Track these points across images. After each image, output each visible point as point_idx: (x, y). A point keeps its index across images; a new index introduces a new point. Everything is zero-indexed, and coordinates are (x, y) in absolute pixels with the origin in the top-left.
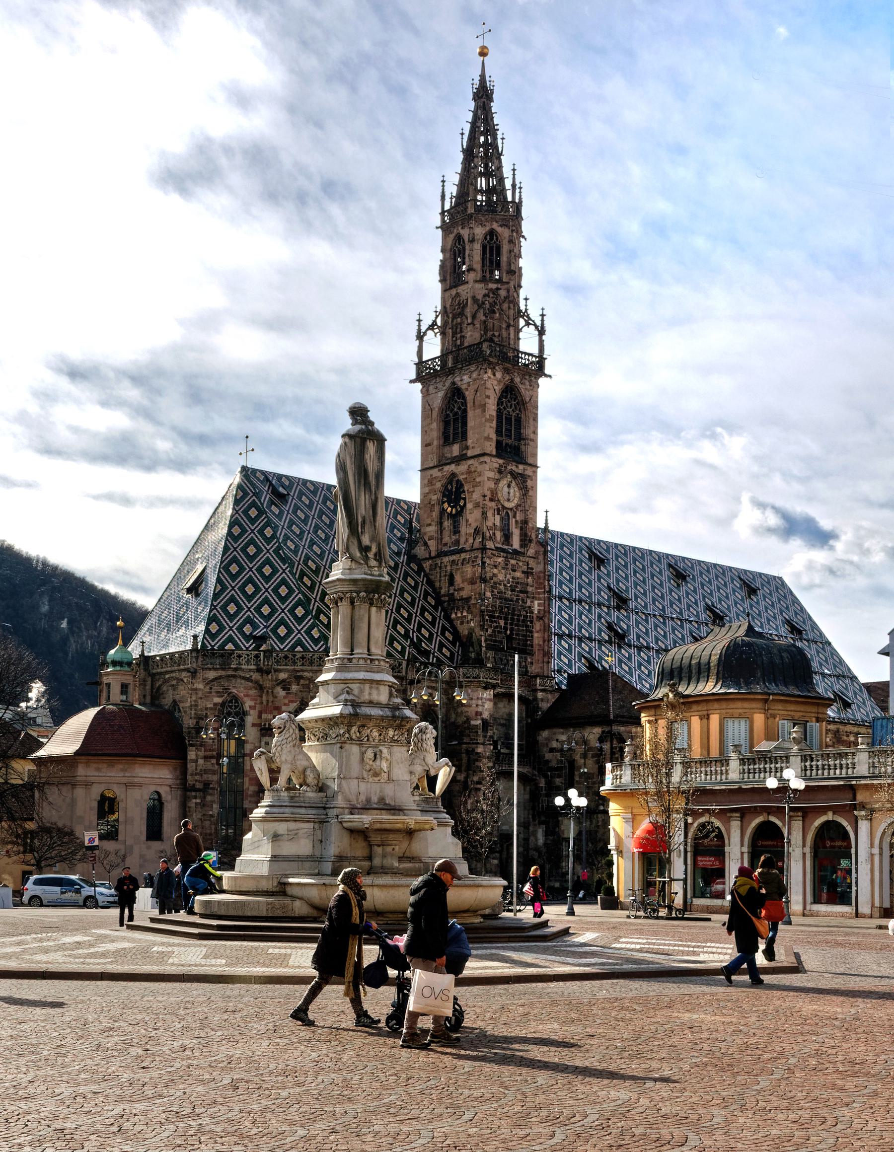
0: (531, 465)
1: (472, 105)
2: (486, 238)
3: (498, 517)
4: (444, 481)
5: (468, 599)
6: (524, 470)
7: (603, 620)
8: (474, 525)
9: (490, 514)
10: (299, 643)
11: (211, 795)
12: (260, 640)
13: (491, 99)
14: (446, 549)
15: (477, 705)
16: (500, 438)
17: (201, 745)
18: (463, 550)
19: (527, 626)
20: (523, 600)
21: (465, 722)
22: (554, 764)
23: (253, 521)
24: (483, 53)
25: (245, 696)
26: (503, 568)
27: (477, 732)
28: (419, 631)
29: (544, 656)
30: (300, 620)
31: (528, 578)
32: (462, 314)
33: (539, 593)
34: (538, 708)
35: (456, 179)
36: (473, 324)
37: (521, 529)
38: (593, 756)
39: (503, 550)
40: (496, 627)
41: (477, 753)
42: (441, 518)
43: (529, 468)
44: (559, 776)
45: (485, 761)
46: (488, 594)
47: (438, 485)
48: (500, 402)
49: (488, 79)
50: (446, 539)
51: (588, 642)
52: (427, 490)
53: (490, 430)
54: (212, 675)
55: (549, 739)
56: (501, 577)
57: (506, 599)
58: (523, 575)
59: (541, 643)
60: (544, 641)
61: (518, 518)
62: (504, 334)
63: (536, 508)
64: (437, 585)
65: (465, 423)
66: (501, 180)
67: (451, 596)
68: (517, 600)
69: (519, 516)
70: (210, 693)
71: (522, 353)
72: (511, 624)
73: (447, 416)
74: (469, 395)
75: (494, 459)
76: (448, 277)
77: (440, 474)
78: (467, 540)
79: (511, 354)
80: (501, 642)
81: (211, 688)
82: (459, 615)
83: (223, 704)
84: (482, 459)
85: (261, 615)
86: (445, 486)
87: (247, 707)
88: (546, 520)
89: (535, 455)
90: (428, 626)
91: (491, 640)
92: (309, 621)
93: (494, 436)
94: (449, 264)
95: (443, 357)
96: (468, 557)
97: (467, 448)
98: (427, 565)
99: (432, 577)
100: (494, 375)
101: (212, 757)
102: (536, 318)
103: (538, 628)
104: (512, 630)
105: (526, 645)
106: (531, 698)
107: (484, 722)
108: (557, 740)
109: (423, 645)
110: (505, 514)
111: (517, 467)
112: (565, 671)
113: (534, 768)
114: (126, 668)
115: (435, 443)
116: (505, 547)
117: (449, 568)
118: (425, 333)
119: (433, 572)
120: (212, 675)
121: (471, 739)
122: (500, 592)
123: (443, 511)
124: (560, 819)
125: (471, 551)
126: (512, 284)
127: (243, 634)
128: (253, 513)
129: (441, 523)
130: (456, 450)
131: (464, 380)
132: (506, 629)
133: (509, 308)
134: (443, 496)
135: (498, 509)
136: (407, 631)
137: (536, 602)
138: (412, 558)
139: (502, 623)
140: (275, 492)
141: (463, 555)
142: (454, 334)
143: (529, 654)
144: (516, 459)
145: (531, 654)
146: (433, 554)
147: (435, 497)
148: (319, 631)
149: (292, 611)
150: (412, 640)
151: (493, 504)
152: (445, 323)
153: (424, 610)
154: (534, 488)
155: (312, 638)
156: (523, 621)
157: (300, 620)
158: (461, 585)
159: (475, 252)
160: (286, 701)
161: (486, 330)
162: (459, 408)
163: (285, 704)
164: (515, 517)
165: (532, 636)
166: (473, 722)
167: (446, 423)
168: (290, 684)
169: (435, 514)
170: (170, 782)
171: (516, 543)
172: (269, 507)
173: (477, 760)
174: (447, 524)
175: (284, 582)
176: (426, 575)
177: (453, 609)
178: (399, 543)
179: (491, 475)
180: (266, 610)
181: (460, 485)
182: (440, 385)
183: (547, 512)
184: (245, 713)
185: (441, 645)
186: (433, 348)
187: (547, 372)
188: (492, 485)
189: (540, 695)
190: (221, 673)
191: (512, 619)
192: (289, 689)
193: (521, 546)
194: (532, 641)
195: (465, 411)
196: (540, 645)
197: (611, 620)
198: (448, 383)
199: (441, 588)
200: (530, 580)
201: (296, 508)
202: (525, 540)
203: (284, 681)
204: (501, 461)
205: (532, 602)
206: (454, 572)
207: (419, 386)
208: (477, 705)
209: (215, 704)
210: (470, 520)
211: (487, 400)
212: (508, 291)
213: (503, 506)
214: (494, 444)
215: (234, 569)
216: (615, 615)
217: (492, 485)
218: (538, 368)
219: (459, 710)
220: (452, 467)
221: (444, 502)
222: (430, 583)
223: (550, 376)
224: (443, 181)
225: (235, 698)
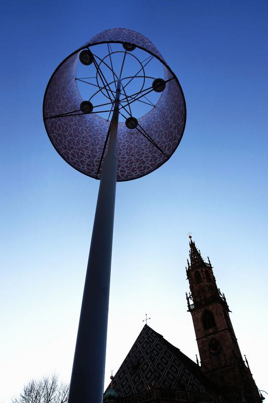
13: (194, 245)
24: (190, 237)
52: (201, 346)
74: (214, 312)
77: (206, 339)
97: (218, 328)
115: (202, 329)
130: (211, 331)
182: (200, 311)
198: (203, 310)
221: (210, 350)
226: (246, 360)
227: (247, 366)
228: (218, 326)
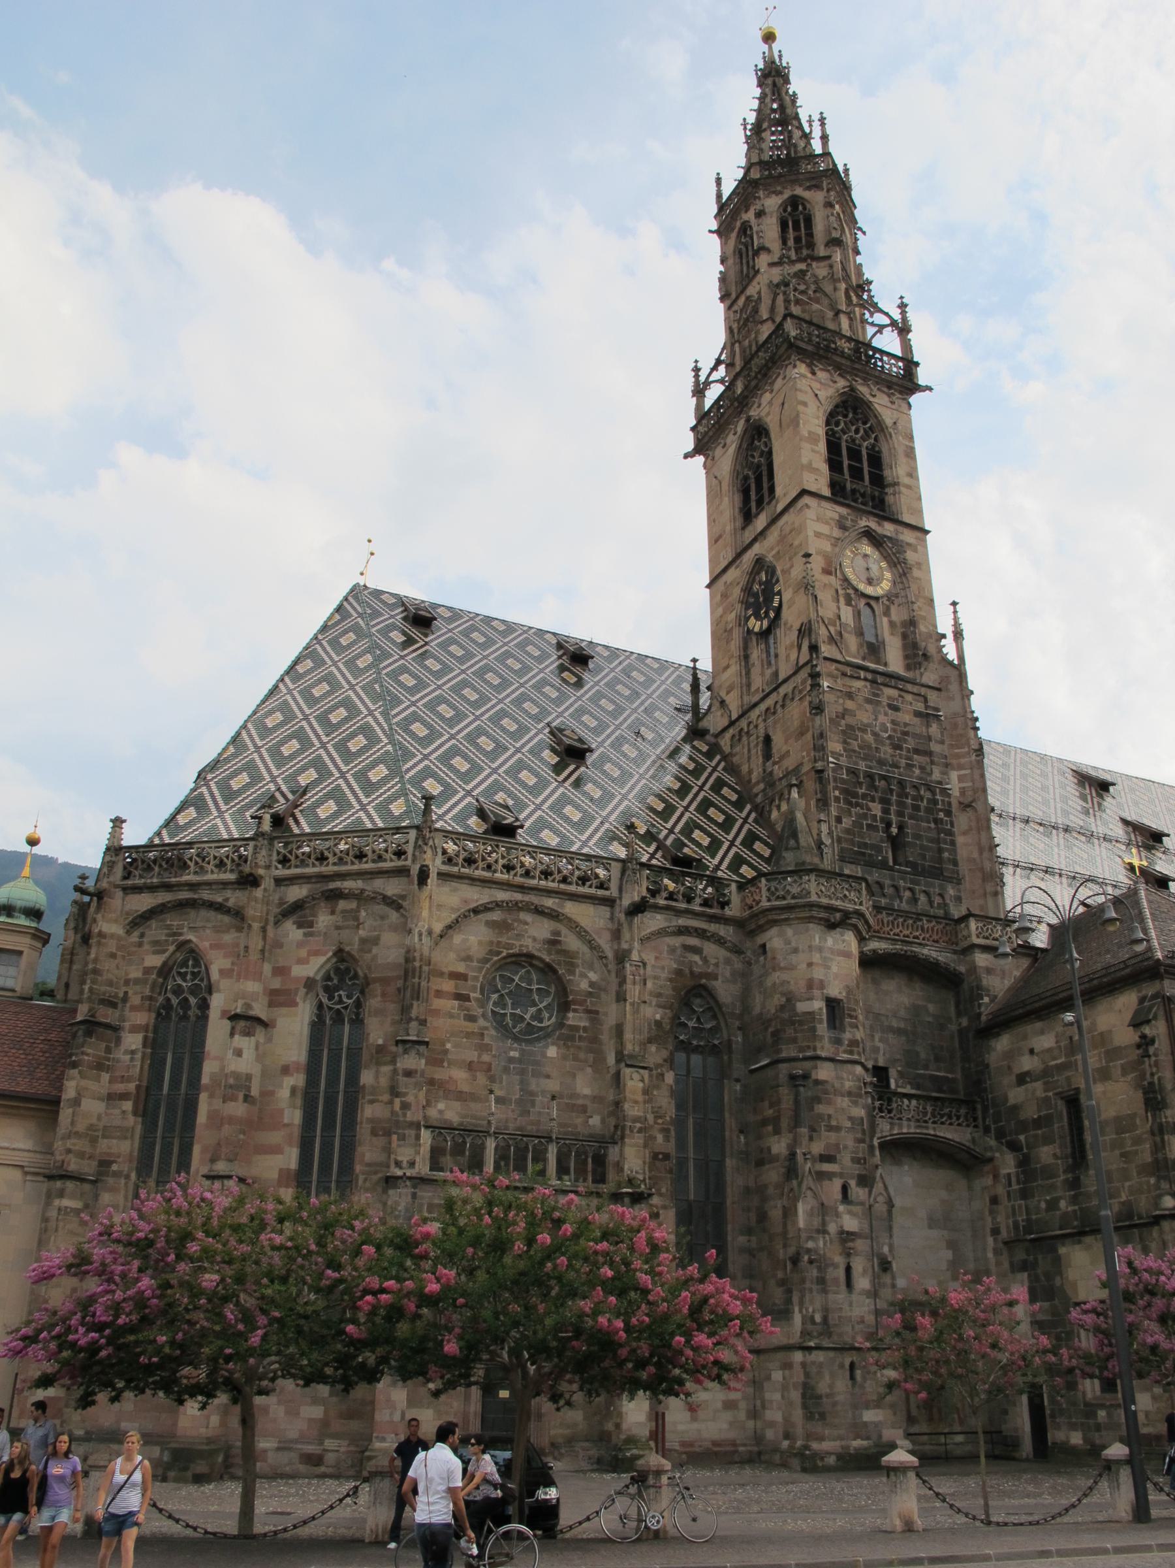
2: (785, 211)
4: (743, 582)
11: (113, 1190)
15: (810, 965)
16: (837, 476)
17: (100, 1066)
19: (937, 821)
20: (922, 768)
21: (782, 1008)
22: (1031, 1112)
25: (212, 947)
26: (868, 701)
27: (814, 1029)
29: (984, 879)
31: (928, 726)
33: (958, 756)
34: (977, 991)
37: (904, 636)
38: (1124, 1073)
40: (865, 816)
41: (817, 1082)
42: (746, 647)
43: (906, 531)
44: (1047, 1140)
45: (843, 1102)
47: (737, 592)
48: (831, 419)
53: (815, 455)
54: (144, 902)
55: (1010, 1055)
57: (881, 763)
58: (917, 720)
59: (976, 855)
60: (981, 852)
61: (894, 617)
63: (932, 600)
64: (745, 769)
67: (769, 779)
69: (898, 614)
70: (140, 945)
72: (900, 814)
73: (746, 478)
75: (825, 504)
78: (788, 656)
80: (879, 849)
81: (142, 935)
83: (164, 971)
86: (748, 590)
87: (215, 975)
88: (956, 619)
89: (919, 512)
91: (852, 842)
94: (732, 277)
96: (791, 688)
98: (725, 742)
99: (736, 760)
100: (814, 373)
101: (124, 1096)
103: (964, 827)
104: (901, 828)
105: (940, 860)
106: (962, 969)
107: (833, 1004)
108: (1032, 1051)
113: (987, 1130)
114: (22, 921)
117: (761, 726)
119: (737, 749)
120: (144, 902)
121: (801, 1050)
122: (865, 746)
124: (1062, 1250)
129: (746, 657)
132: (889, 825)
139: (876, 809)
143: (949, 880)
145: (957, 881)
154: (924, 565)
156: (928, 810)
158: (785, 749)
159: (769, 231)
160: (303, 953)
163: (302, 961)
164: (887, 613)
165: (953, 843)
166: (802, 1007)
167: (745, 492)
170: (23, 1159)
171: (895, 660)
173: (818, 1100)
176: (724, 758)
177: (773, 800)
179: (825, 529)
183: (954, 604)
187: (922, 380)
189: (982, 959)
191: (901, 804)
192: (312, 927)
193: (908, 668)
194: (954, 851)
196: (971, 860)
198: (741, 425)
199: (750, 772)
200: (934, 729)
202: (916, 655)
207: (700, 459)
208: (810, 965)
209: (147, 971)
213: (856, 590)
217: (827, 547)
219: (769, 983)
221: (747, 619)
222: (732, 769)
223: (930, 389)
225: (192, 956)
226: (956, 624)
227: (952, 656)
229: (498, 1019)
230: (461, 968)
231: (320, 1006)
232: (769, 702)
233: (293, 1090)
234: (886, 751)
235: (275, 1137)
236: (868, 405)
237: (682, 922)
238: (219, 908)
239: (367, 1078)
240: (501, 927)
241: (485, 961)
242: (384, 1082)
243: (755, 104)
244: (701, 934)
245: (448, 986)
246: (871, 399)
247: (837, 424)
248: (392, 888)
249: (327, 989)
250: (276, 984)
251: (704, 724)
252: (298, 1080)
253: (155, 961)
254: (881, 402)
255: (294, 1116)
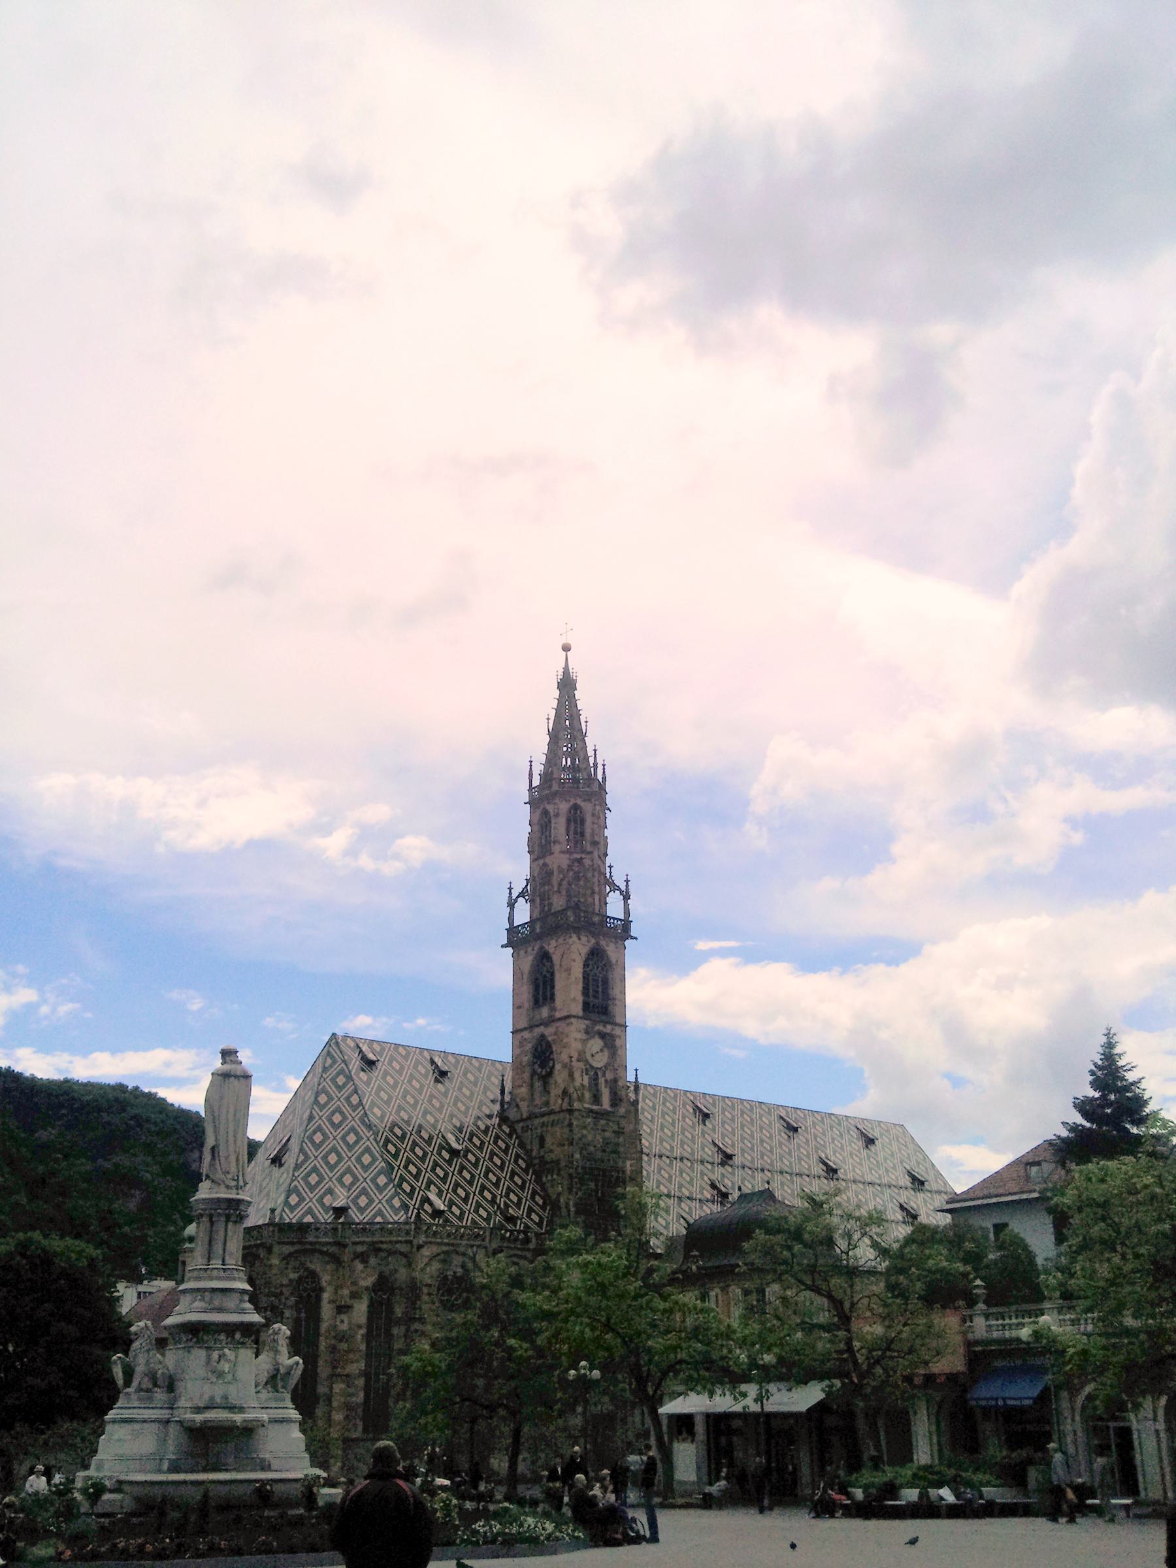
0: (621, 1025)
1: (557, 693)
3: (586, 1078)
5: (557, 1162)
6: (613, 1029)
7: (706, 1178)
8: (562, 1086)
9: (577, 1075)
10: (380, 1213)
12: (340, 1211)
14: (537, 1110)
18: (552, 1112)
23: (340, 1088)
24: (566, 648)
26: (592, 1129)
28: (507, 1196)
30: (380, 1189)
32: (549, 883)
35: (543, 759)
36: (559, 892)
39: (591, 1111)
42: (532, 1079)
46: (577, 1156)
47: (529, 1046)
48: (586, 965)
49: (571, 671)
50: (538, 1102)
51: (689, 1202)
53: (576, 992)
54: (287, 1249)
56: (590, 1137)
62: (590, 900)
64: (529, 1147)
65: (553, 987)
66: (587, 758)
68: (609, 1160)
69: (609, 1076)
71: (611, 918)
73: (537, 979)
74: (556, 958)
76: (536, 848)
78: (556, 1101)
79: (596, 919)
81: (288, 1263)
82: (549, 1178)
84: (568, 1021)
85: (342, 1184)
87: (324, 1284)
90: (517, 1190)
92: (390, 1190)
93: (580, 998)
95: (532, 922)
98: (519, 1127)
100: (579, 939)
102: (620, 882)
109: (511, 1211)
110: (595, 1075)
111: (605, 1026)
112: (661, 1234)
115: (526, 1005)
116: (594, 1107)
118: (516, 901)
119: (526, 1134)
120: (287, 1249)
122: (591, 1154)
123: (533, 1073)
125: (559, 1112)
126: (596, 854)
127: (322, 1204)
128: (341, 1080)
130: (545, 1012)
131: (551, 946)
133: (593, 876)
134: (534, 1057)
135: (586, 1069)
136: (494, 1197)
137: (628, 1163)
138: (503, 1119)
139: (592, 1185)
140: (364, 1059)
141: (552, 1117)
142: (542, 900)
144: (603, 1018)
146: (524, 1116)
147: (525, 1059)
148: (400, 1199)
149: (374, 1180)
150: (499, 1207)
151: (581, 1065)
152: (534, 890)
153: (513, 1173)
155: (392, 1206)
157: (380, 1189)
158: (552, 1147)
161: (569, 896)
162: (548, 972)
163: (364, 1279)
164: (604, 1075)
167: (536, 989)
168: (368, 1256)
169: (527, 1076)
172: (357, 1074)
174: (538, 1084)
175: (367, 1150)
178: (491, 1105)
180: (348, 1179)
181: (549, 1045)
182: (530, 949)
183: (636, 1070)
184: (322, 1290)
185: (530, 1210)
186: (523, 913)
188: (579, 1046)
190: (297, 1247)
193: (612, 1106)
195: (552, 974)
197: (714, 1178)
199: (532, 1150)
200: (621, 1139)
201: (386, 1073)
203: (362, 1253)
204: (587, 1022)
205: (624, 1162)
206: (544, 1134)
207: (510, 950)
210: (559, 1081)
211: (573, 963)
212: (592, 861)
214: (580, 1006)
215: (318, 1138)
216: (717, 1173)
217: (579, 1046)
218: (624, 930)
220: (541, 1029)
221: (535, 1063)
222: (522, 1145)
223: (636, 938)
224: (531, 762)
225: (313, 1275)
228: (558, 1002)
229: (441, 1301)
230: (429, 1281)
231: (372, 1298)
232: (545, 1119)
233: (363, 1335)
234: (599, 1155)
235: (357, 1356)
236: (605, 951)
237: (512, 1252)
238: (322, 1253)
239: (395, 1331)
240: (444, 1261)
241: (438, 1277)
242: (402, 1334)
243: (555, 704)
244: (520, 1257)
245: (425, 1290)
246: (606, 948)
247: (588, 965)
248: (403, 1248)
249: (374, 1291)
250: (354, 1289)
251: (506, 1114)
252: (363, 1331)
253: (294, 1276)
254: (610, 949)
255: (363, 1347)
